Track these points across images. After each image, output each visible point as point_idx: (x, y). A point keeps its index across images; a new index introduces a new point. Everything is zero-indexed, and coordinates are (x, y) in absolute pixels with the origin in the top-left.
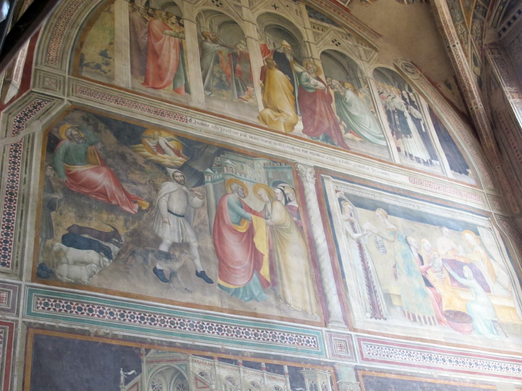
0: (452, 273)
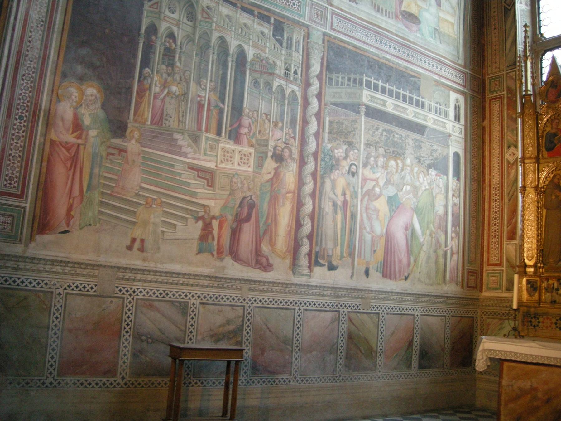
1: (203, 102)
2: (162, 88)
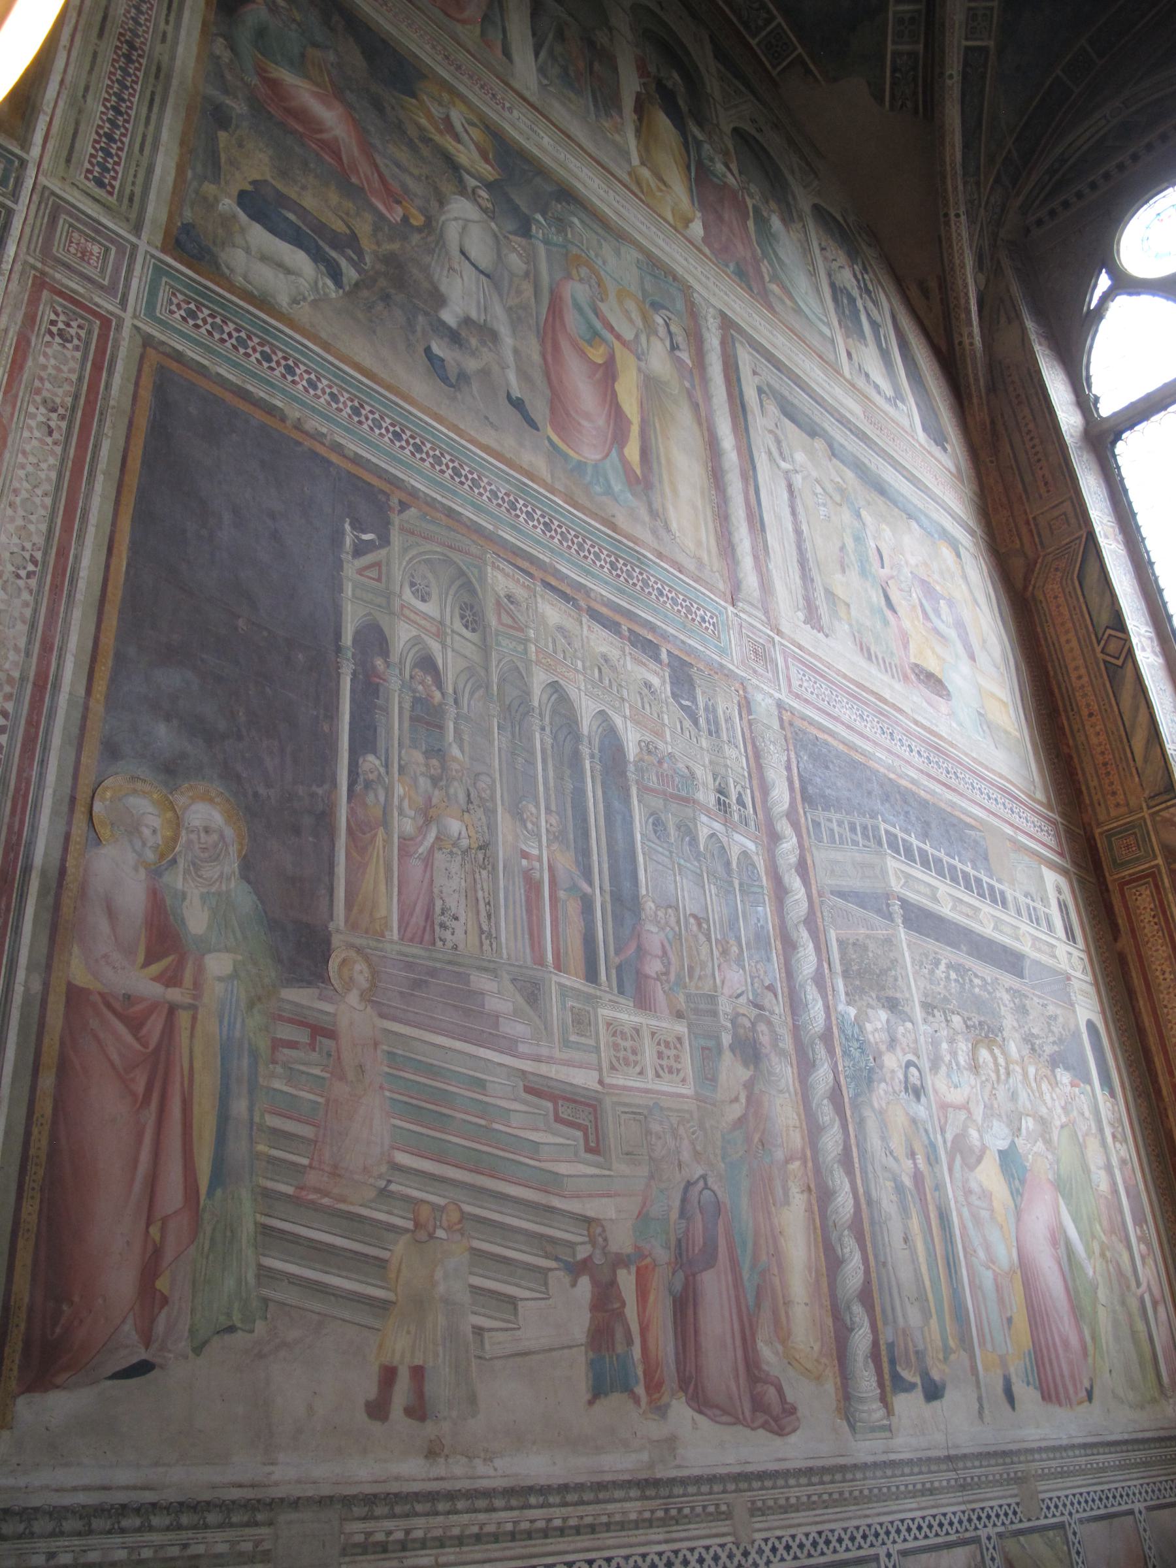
0: (924, 601)
2: (421, 822)
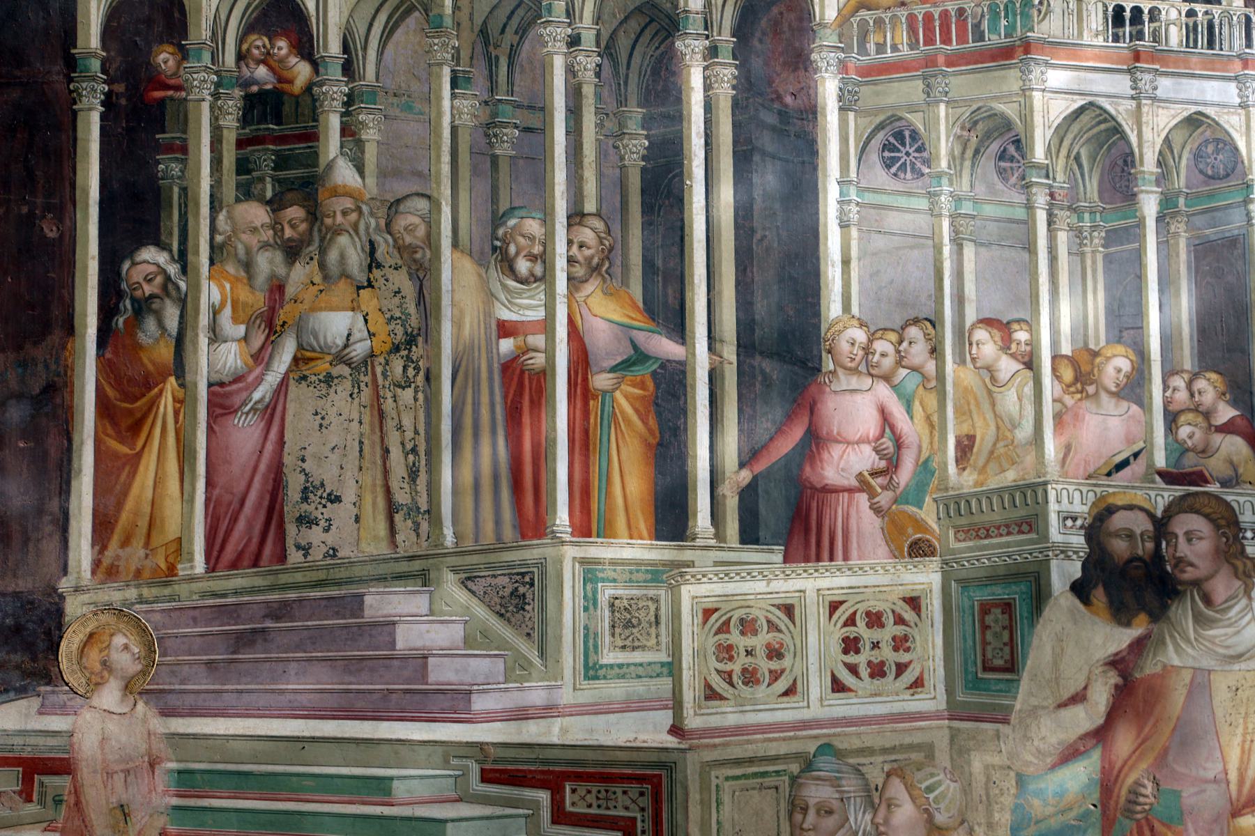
1: (539, 360)
2: (258, 339)
